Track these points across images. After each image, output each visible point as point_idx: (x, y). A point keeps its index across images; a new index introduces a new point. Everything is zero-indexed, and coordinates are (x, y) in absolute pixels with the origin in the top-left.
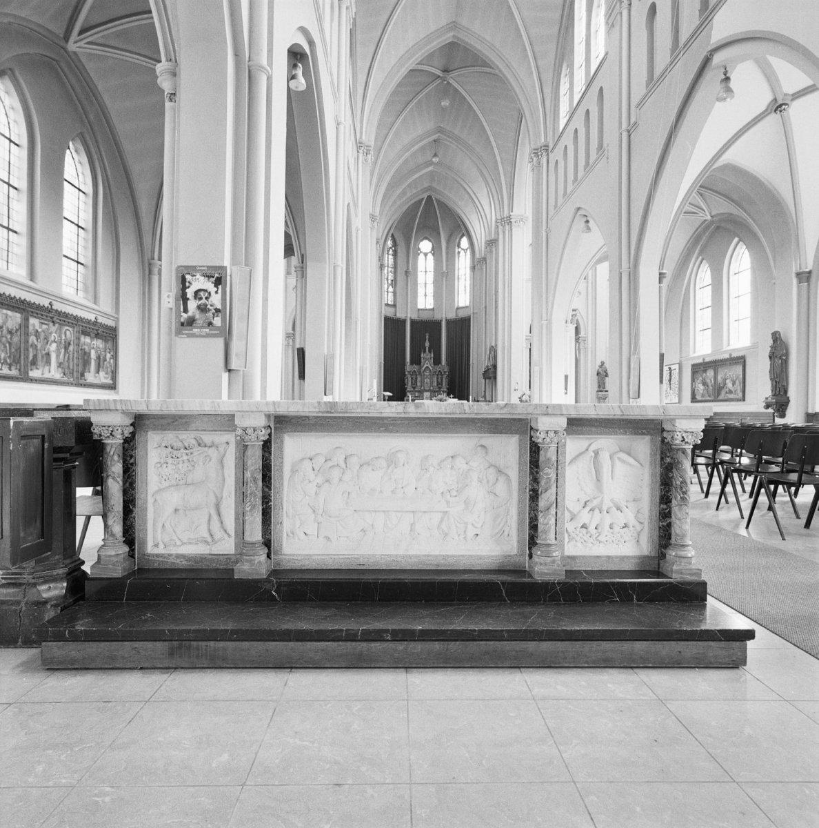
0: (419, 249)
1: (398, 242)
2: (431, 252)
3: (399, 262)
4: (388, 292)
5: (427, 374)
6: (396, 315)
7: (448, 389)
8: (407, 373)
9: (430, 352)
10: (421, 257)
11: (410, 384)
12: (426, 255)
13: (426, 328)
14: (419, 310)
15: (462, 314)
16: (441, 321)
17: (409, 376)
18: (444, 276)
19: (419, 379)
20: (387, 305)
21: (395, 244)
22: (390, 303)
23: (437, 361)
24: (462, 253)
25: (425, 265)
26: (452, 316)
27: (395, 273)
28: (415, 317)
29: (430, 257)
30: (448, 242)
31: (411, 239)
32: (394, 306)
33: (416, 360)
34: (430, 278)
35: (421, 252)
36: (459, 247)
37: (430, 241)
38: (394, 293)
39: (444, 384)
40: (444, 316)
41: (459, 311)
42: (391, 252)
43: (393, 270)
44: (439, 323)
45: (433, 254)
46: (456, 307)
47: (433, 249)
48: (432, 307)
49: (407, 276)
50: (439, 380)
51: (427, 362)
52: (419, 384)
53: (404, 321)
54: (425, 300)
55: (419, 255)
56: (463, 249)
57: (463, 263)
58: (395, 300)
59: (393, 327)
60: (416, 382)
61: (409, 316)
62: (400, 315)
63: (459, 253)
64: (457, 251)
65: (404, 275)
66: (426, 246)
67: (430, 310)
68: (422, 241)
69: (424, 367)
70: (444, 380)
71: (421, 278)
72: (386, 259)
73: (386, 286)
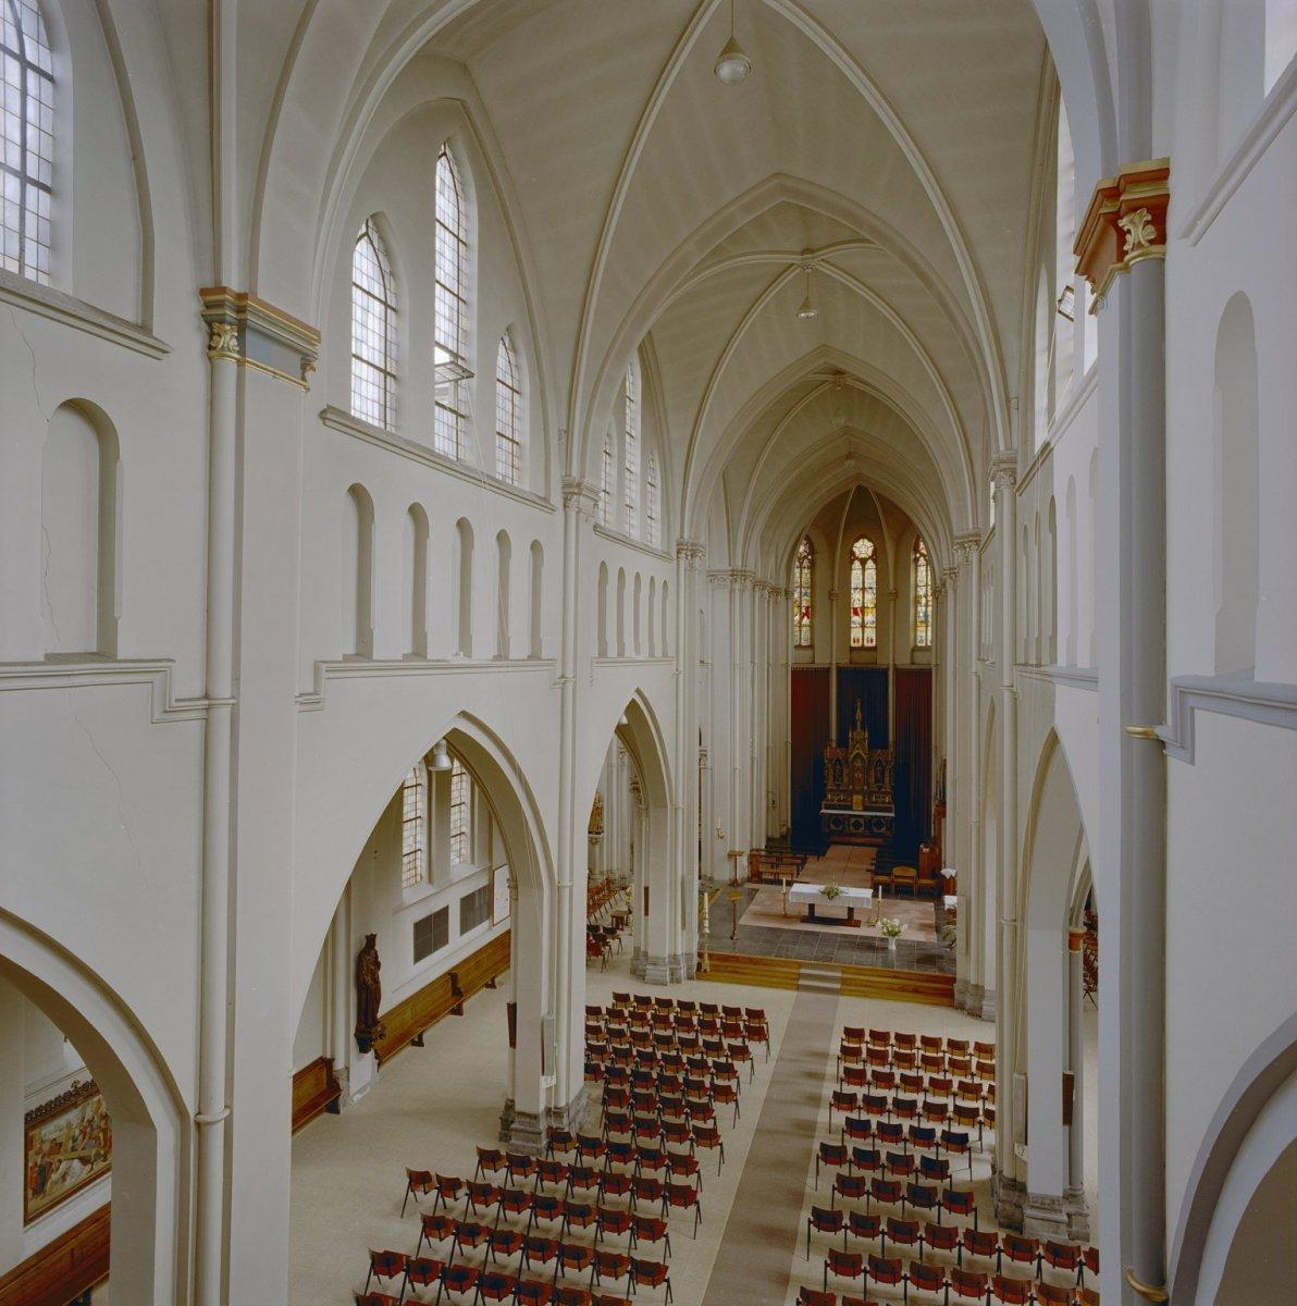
0: (853, 553)
1: (816, 546)
2: (870, 558)
3: (818, 578)
4: (800, 627)
5: (858, 764)
6: (813, 662)
7: (892, 788)
8: (826, 761)
9: (863, 728)
10: (857, 564)
11: (831, 778)
12: (863, 562)
13: (863, 683)
14: (852, 649)
15: (921, 658)
16: (887, 669)
17: (829, 765)
18: (892, 597)
19: (845, 772)
20: (799, 647)
21: (812, 551)
22: (804, 643)
23: (878, 740)
24: (922, 561)
25: (863, 580)
26: (904, 661)
27: (812, 595)
28: (845, 661)
29: (870, 564)
30: (898, 543)
31: (836, 543)
32: (811, 647)
33: (843, 742)
34: (870, 598)
35: (857, 558)
36: (916, 550)
37: (870, 540)
38: (811, 626)
39: (887, 780)
40: (891, 663)
41: (917, 654)
42: (806, 563)
43: (809, 591)
44: (885, 672)
45: (875, 561)
46: (912, 647)
47: (874, 552)
48: (874, 644)
49: (832, 600)
50: (879, 775)
51: (858, 745)
52: (845, 779)
53: (827, 671)
54: (864, 632)
55: (852, 562)
56: (922, 555)
57: (923, 575)
58: (812, 638)
59: (806, 685)
60: (841, 775)
61: (834, 662)
62: (821, 660)
63: (916, 560)
64: (913, 557)
65: (832, 598)
66: (863, 548)
67: (870, 649)
68: (857, 541)
69: (854, 753)
70: (887, 774)
71: (856, 597)
72: (798, 575)
73: (797, 618)
